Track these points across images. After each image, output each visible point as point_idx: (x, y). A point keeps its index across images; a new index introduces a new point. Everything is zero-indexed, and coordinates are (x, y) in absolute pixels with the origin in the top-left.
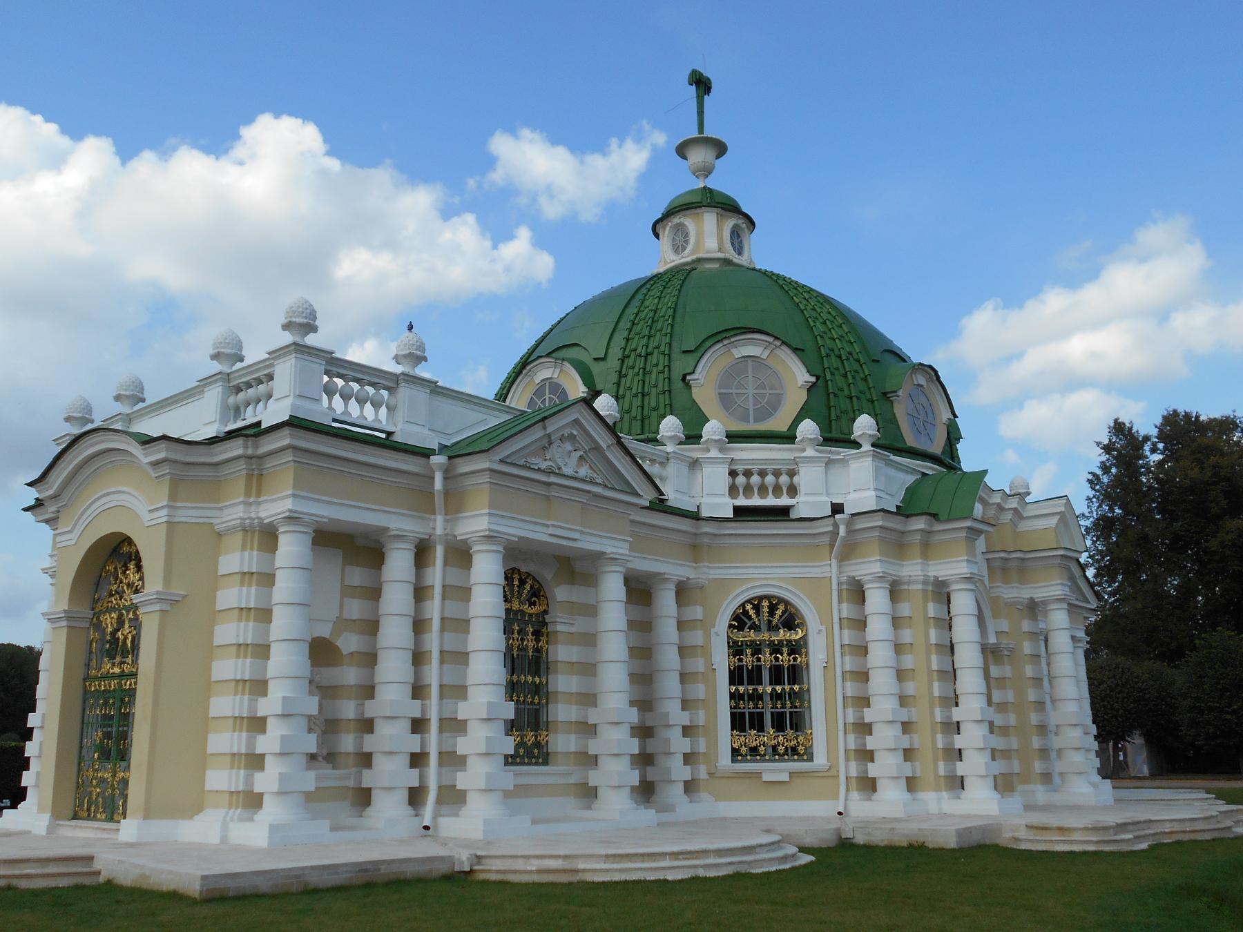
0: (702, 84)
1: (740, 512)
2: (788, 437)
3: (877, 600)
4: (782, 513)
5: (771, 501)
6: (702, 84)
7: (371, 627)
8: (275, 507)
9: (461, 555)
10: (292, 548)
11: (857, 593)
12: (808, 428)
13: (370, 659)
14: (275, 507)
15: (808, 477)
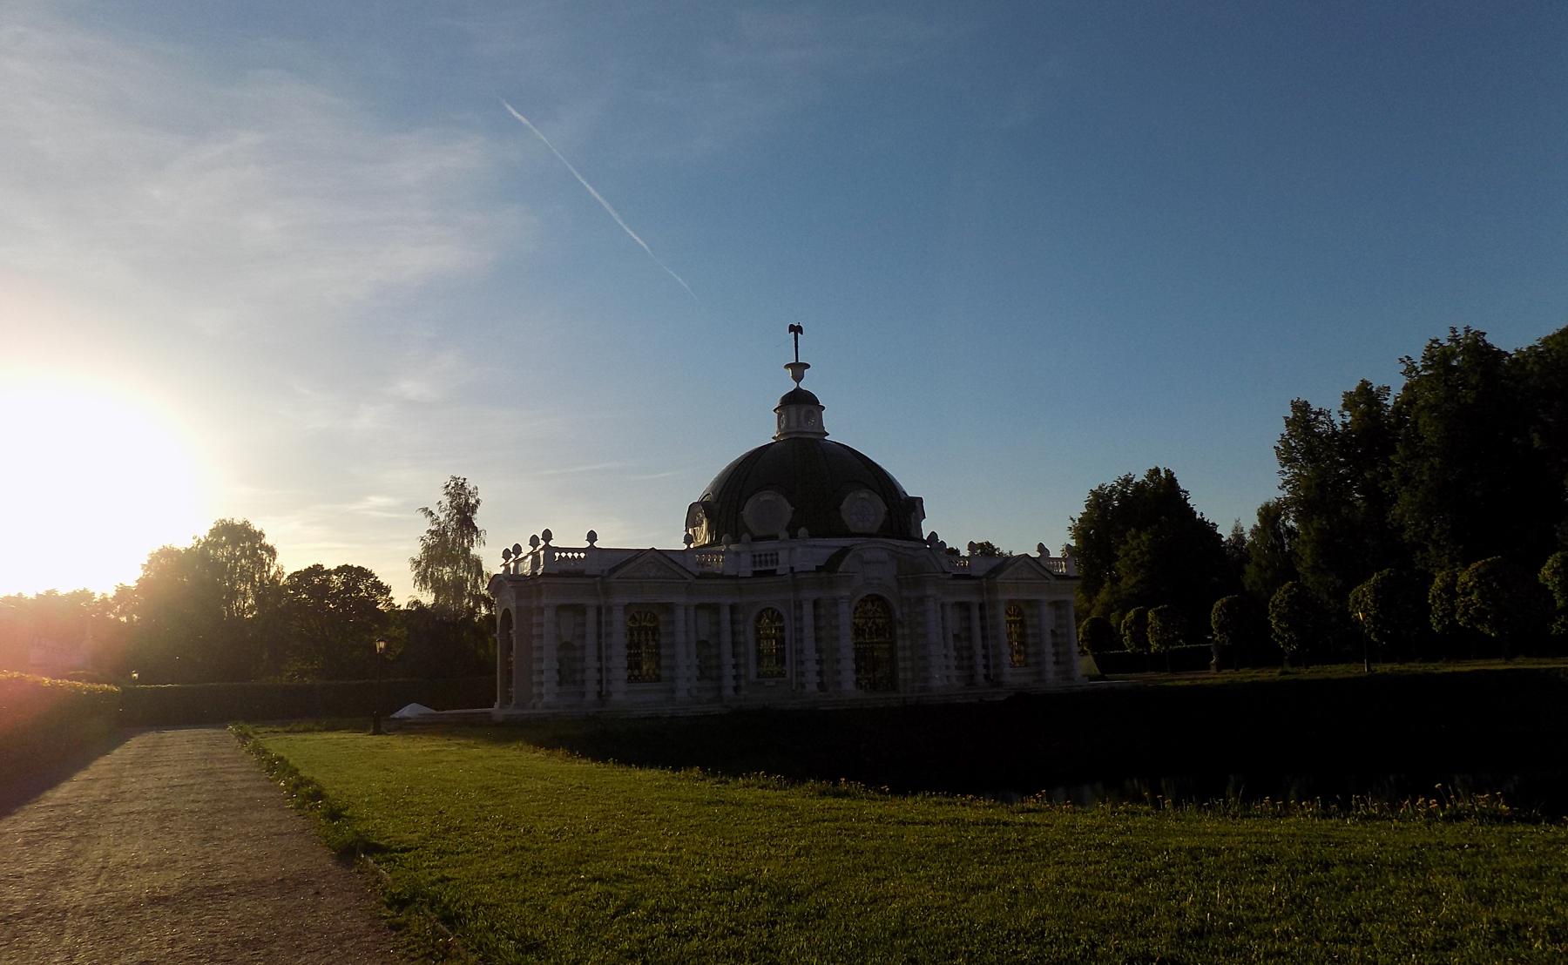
0: (796, 330)
1: (756, 574)
2: (774, 537)
3: (808, 609)
4: (772, 573)
5: (770, 568)
6: (796, 330)
7: (583, 637)
8: (544, 601)
9: (610, 610)
10: (549, 614)
11: (799, 606)
12: (784, 535)
13: (583, 647)
14: (544, 601)
15: (783, 556)
